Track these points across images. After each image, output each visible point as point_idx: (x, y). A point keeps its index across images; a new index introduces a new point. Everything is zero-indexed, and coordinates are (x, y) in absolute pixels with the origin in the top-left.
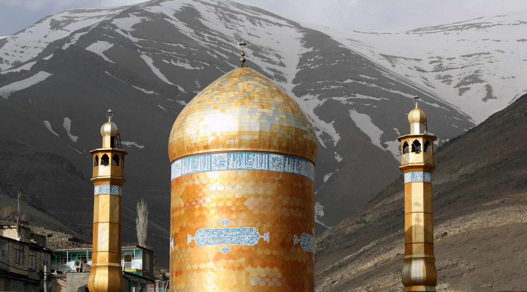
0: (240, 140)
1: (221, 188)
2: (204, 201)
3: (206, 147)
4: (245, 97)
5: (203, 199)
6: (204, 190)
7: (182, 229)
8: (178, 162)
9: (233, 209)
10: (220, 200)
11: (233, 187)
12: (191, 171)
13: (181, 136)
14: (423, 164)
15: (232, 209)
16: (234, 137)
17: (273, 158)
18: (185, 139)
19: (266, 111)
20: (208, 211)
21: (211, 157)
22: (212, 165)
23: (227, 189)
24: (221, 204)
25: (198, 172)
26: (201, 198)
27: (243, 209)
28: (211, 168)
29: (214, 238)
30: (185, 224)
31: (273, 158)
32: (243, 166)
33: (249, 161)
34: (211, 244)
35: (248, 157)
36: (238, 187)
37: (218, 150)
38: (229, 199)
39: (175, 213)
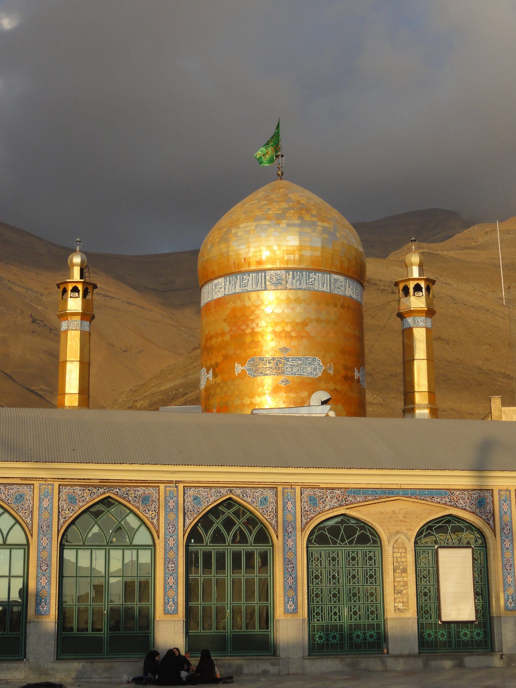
0: (301, 256)
1: (278, 311)
2: (257, 324)
3: (259, 263)
4: (301, 209)
5: (256, 322)
6: (258, 312)
7: (226, 358)
8: (221, 280)
9: (293, 334)
10: (276, 324)
11: (293, 309)
12: (238, 290)
13: (224, 250)
14: (426, 309)
15: (292, 334)
16: (293, 253)
17: (335, 279)
18: (231, 254)
19: (326, 225)
20: (263, 336)
21: (265, 274)
22: (268, 283)
23: (286, 311)
24: (278, 329)
25: (248, 291)
26: (253, 321)
27: (305, 334)
28: (265, 287)
29: (271, 368)
30: (231, 352)
31: (335, 279)
32: (304, 286)
33: (311, 280)
34: (267, 375)
35: (309, 276)
36: (298, 309)
37: (274, 266)
38: (287, 324)
39: (214, 340)
